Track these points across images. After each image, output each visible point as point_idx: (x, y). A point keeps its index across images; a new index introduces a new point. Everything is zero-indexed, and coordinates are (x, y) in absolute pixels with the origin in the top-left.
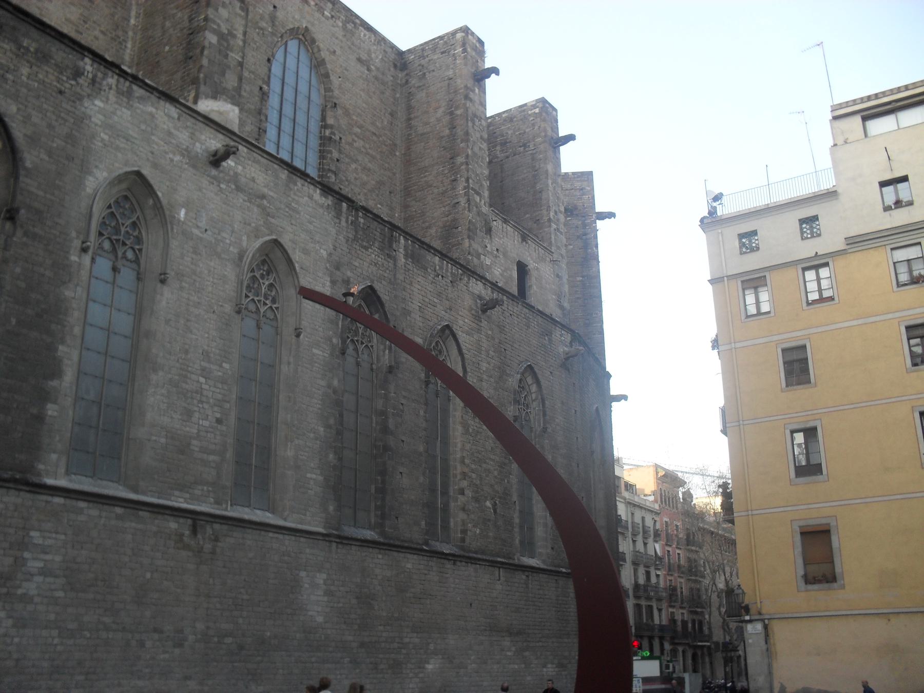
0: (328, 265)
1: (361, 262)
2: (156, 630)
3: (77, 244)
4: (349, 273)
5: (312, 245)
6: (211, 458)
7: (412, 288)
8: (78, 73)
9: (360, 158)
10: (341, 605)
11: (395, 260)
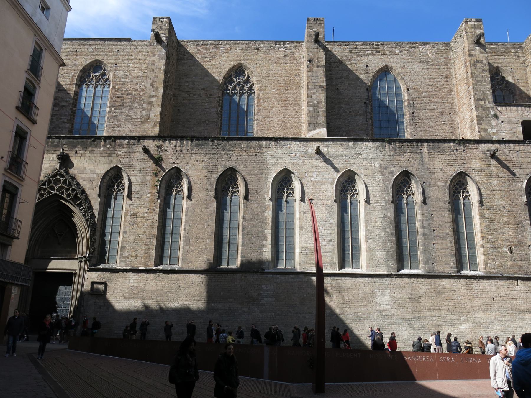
1: (399, 162)
2: (309, 313)
4: (393, 169)
6: (328, 254)
7: (434, 162)
8: (261, 146)
9: (427, 106)
10: (400, 301)
11: (421, 154)
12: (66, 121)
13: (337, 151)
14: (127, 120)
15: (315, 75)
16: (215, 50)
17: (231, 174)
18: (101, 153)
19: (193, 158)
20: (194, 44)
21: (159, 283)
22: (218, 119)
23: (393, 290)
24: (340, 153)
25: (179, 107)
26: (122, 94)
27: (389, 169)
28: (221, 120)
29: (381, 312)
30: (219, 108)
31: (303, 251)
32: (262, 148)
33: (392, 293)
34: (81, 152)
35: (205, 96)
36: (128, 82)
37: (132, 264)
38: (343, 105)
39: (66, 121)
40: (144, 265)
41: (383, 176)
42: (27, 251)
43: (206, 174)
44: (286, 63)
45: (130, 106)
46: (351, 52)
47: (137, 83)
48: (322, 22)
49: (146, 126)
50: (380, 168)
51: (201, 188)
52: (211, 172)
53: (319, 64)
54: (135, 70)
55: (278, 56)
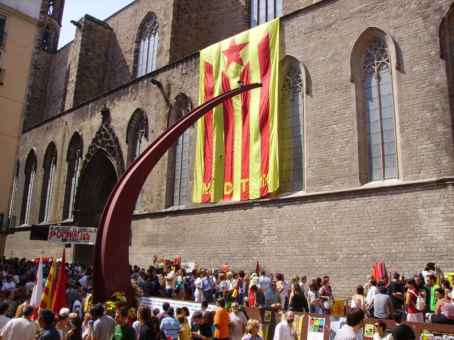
6: (344, 163)
23: (449, 208)
31: (312, 165)
33: (448, 211)
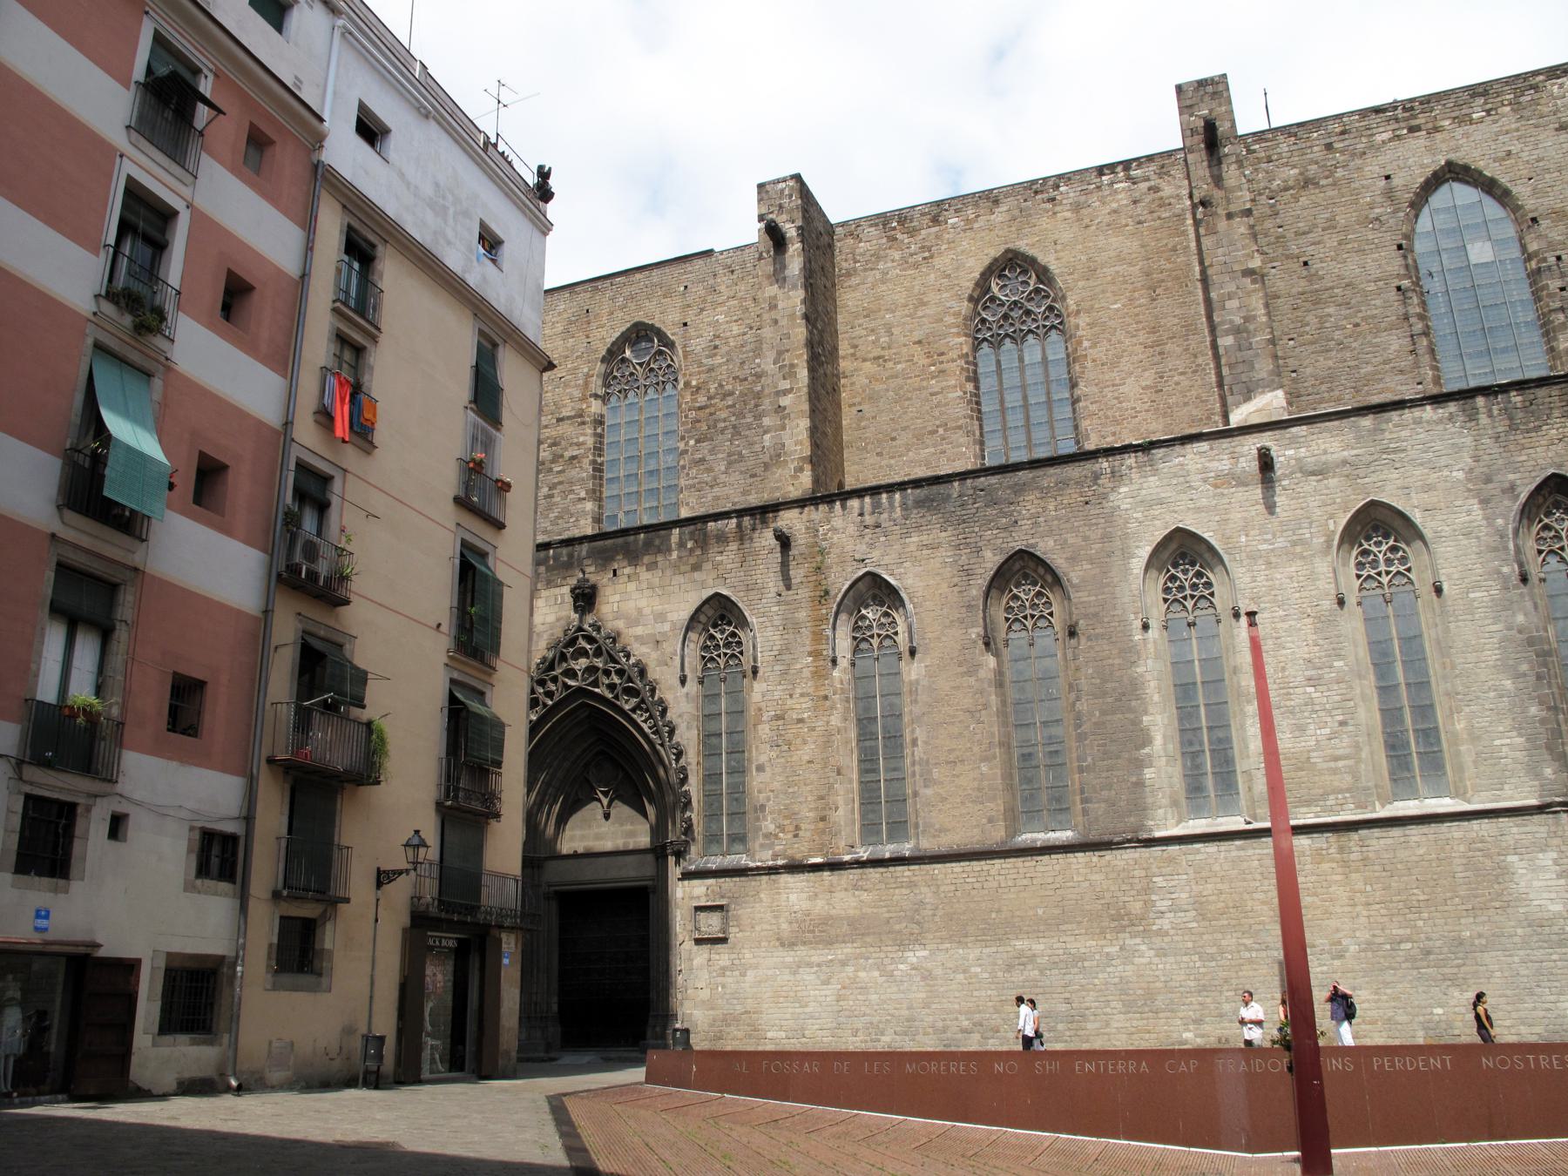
0: (1470, 486)
3: (1138, 624)
4: (1511, 477)
5: (1435, 475)
6: (1341, 764)
8: (1096, 477)
12: (583, 494)
13: (1325, 452)
14: (730, 464)
15: (1224, 242)
16: (937, 228)
17: (1023, 568)
18: (676, 567)
19: (913, 539)
20: (877, 225)
21: (864, 896)
22: (972, 418)
24: (1335, 456)
25: (860, 404)
26: (710, 398)
27: (1499, 477)
28: (980, 419)
29: (1538, 924)
30: (970, 387)
32: (1100, 482)
34: (627, 570)
35: (926, 362)
36: (720, 365)
37: (789, 852)
38: (1331, 310)
39: (583, 494)
40: (820, 850)
41: (1484, 502)
42: (525, 844)
43: (956, 580)
44: (1140, 223)
45: (734, 427)
46: (1329, 147)
47: (743, 363)
48: (1221, 88)
49: (780, 472)
50: (1469, 480)
51: (947, 622)
52: (967, 572)
53: (1233, 208)
54: (735, 328)
55: (1115, 205)
